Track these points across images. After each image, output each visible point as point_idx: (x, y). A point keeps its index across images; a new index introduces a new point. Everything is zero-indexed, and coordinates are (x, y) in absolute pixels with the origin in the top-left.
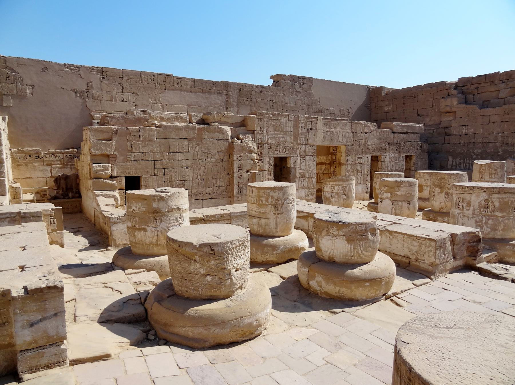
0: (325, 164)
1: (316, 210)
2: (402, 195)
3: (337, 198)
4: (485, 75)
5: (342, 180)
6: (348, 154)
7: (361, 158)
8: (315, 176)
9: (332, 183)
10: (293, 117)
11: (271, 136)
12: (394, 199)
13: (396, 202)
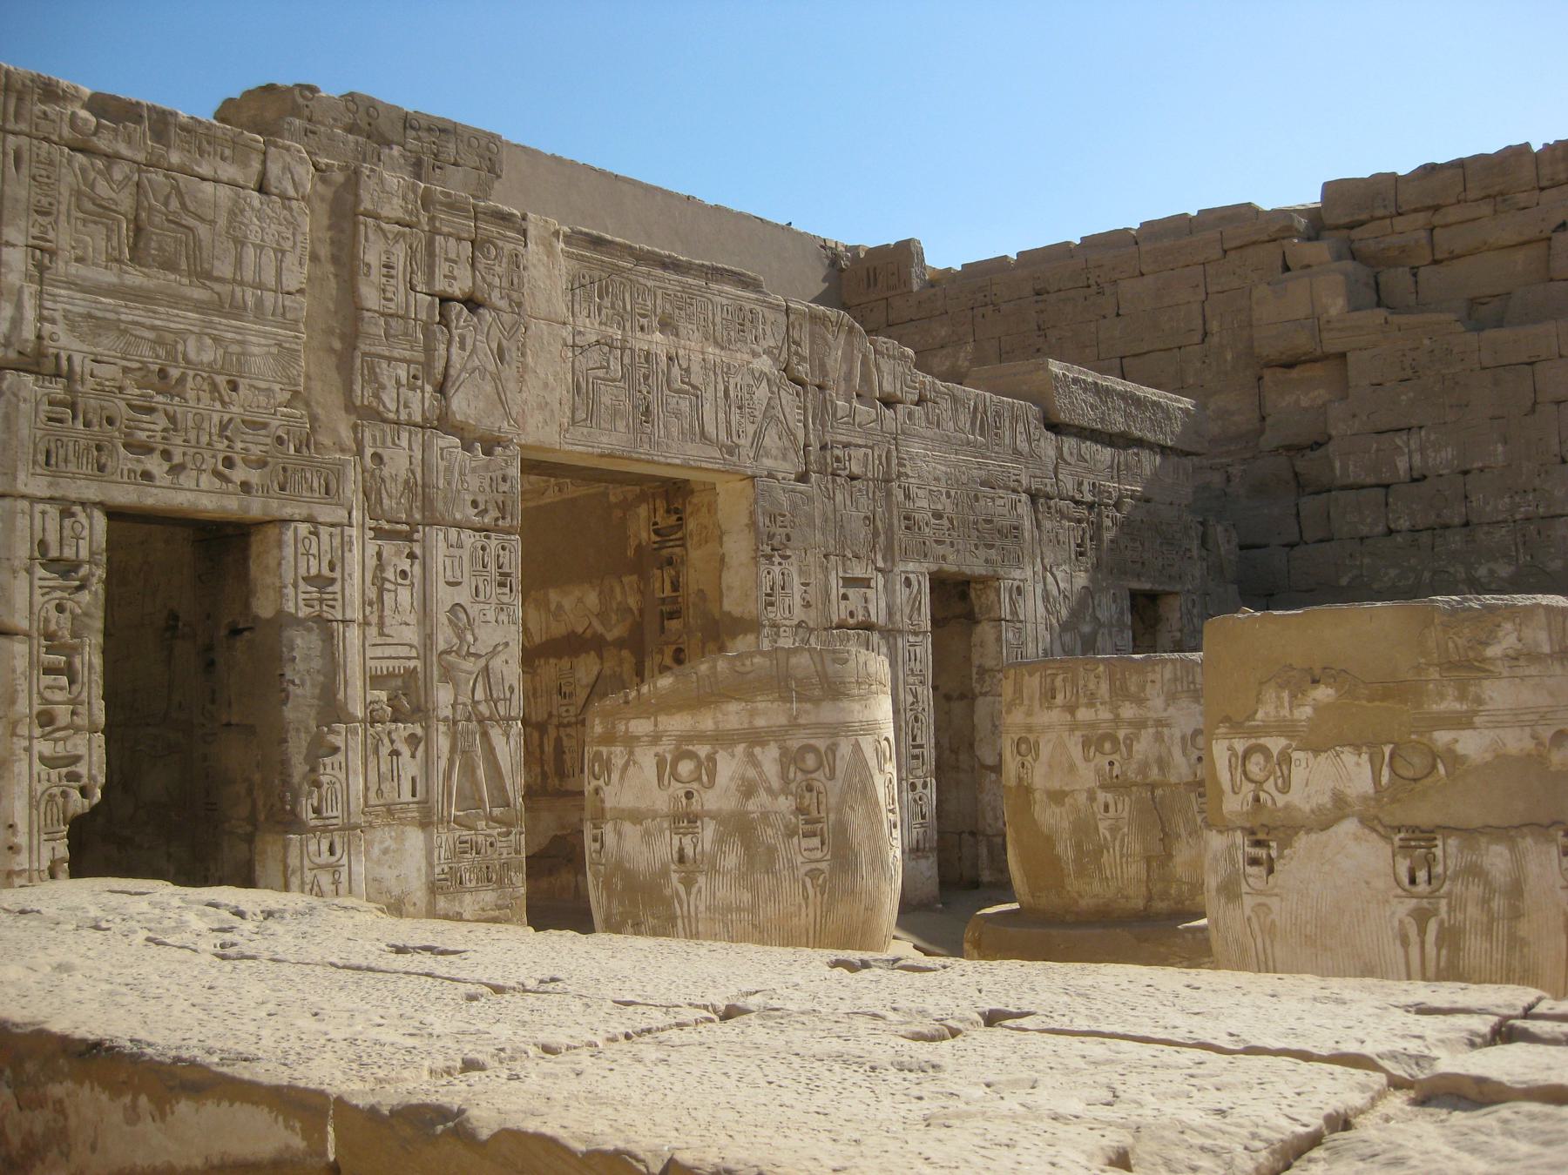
0: (596, 644)
1: (500, 1026)
2: (1502, 760)
4: (1460, 164)
5: (782, 685)
6: (771, 544)
7: (865, 583)
9: (677, 723)
10: (306, 174)
11: (80, 304)
12: (1424, 814)
13: (1448, 851)
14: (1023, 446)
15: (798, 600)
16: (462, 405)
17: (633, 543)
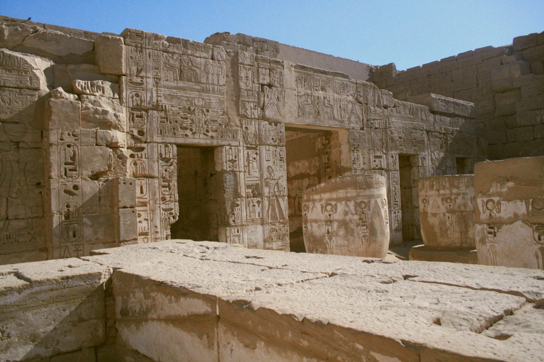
0: (307, 176)
1: (268, 278)
3: (345, 237)
5: (355, 185)
6: (354, 147)
7: (380, 157)
8: (286, 193)
9: (326, 196)
10: (224, 54)
11: (167, 92)
14: (424, 118)
15: (362, 162)
16: (269, 113)
17: (317, 148)
